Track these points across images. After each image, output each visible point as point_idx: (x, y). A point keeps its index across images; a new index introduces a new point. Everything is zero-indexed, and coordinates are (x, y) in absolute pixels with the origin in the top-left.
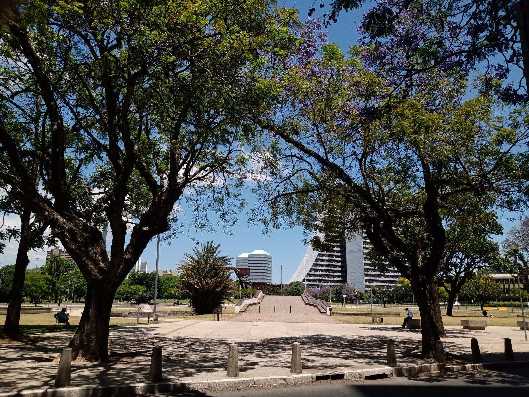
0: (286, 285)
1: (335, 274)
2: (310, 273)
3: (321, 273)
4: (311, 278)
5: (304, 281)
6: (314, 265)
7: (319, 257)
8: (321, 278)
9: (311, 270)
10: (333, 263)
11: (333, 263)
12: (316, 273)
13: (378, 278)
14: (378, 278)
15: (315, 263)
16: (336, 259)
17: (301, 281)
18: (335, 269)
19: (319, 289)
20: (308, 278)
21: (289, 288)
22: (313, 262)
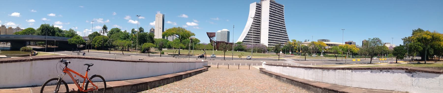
0: (235, 43)
1: (256, 39)
2: (245, 38)
3: (250, 38)
4: (246, 41)
5: (243, 41)
6: (247, 35)
7: (250, 31)
8: (250, 41)
9: (246, 37)
10: (255, 34)
11: (255, 34)
12: (248, 38)
13: (273, 41)
14: (273, 41)
15: (248, 34)
16: (257, 32)
17: (242, 41)
18: (256, 37)
19: (250, 45)
20: (245, 40)
21: (237, 45)
22: (247, 33)
